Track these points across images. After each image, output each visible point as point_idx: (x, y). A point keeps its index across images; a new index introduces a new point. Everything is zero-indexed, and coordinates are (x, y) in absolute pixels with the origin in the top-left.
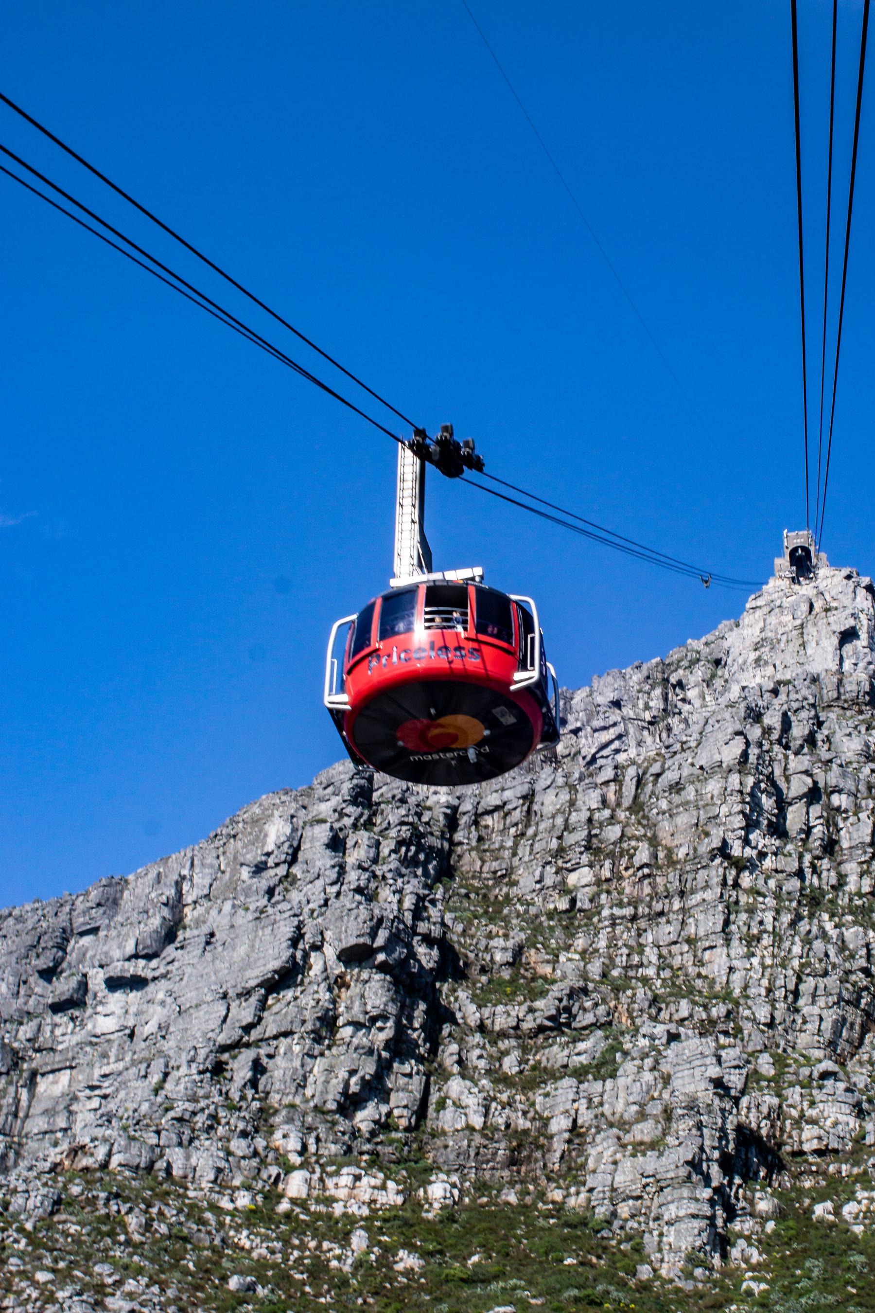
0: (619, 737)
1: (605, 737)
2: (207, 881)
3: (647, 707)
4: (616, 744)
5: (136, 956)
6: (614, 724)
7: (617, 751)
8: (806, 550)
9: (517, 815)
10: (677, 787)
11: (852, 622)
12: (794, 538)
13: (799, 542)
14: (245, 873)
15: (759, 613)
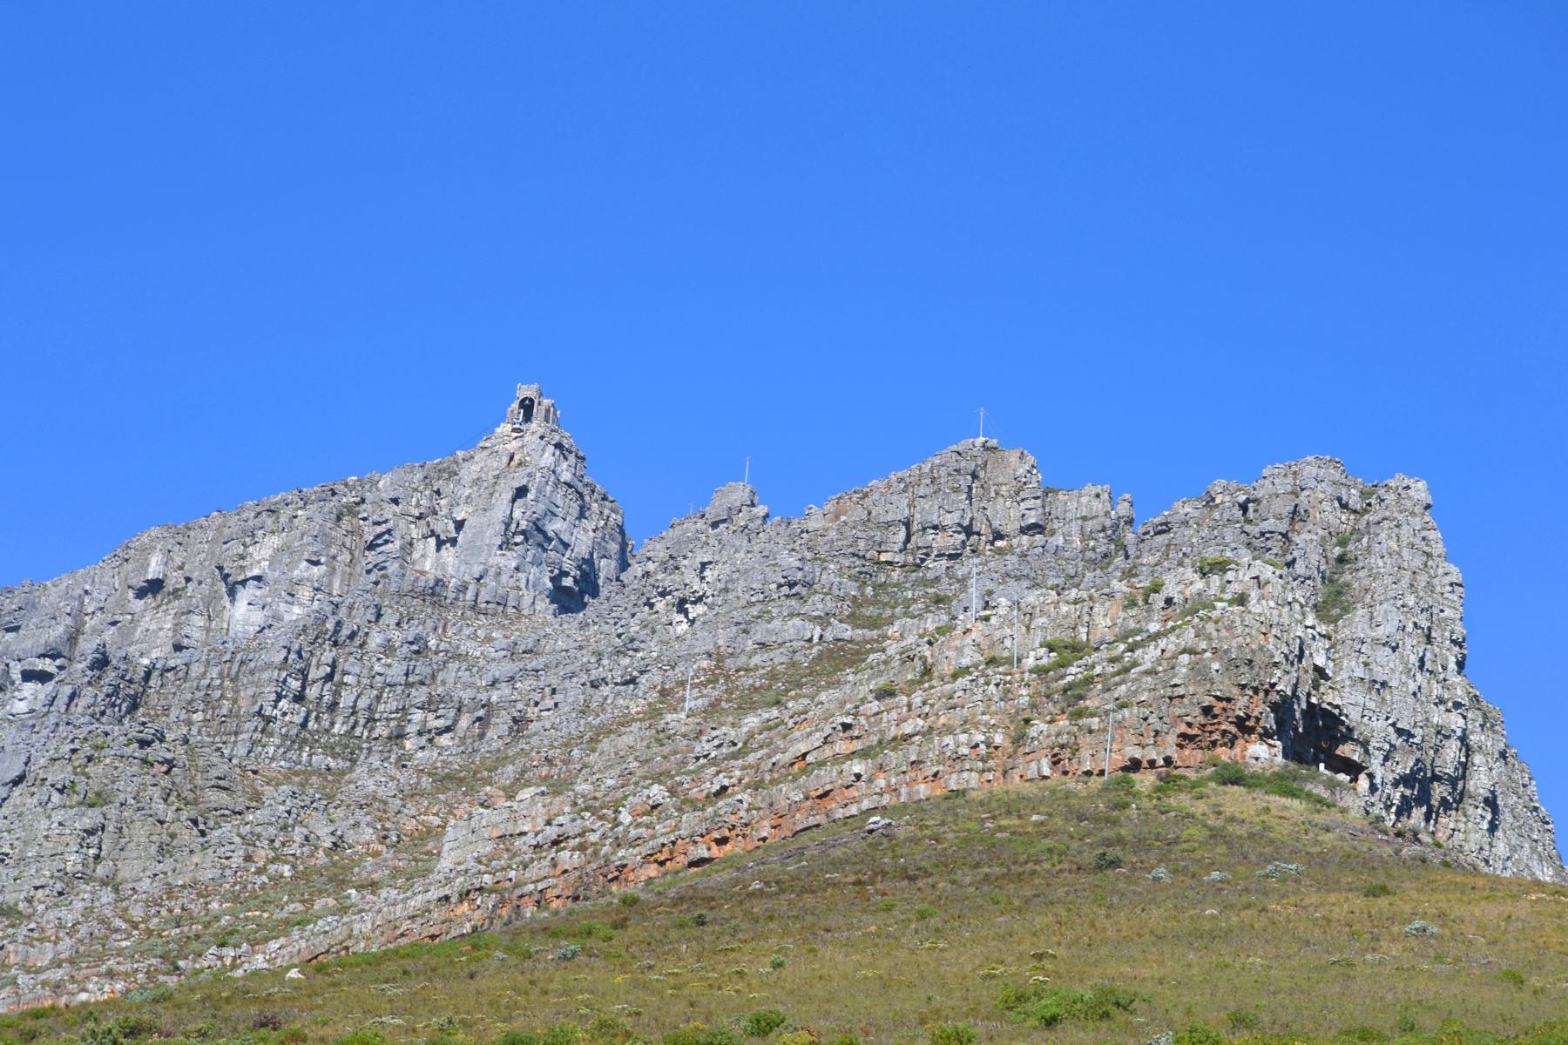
0: (389, 532)
1: (379, 529)
2: (103, 597)
3: (418, 505)
4: (386, 537)
5: (44, 656)
6: (386, 521)
7: (387, 542)
8: (531, 400)
9: (181, 674)
10: (252, 673)
11: (524, 482)
12: (526, 391)
13: (528, 394)
14: (131, 594)
15: (485, 453)
